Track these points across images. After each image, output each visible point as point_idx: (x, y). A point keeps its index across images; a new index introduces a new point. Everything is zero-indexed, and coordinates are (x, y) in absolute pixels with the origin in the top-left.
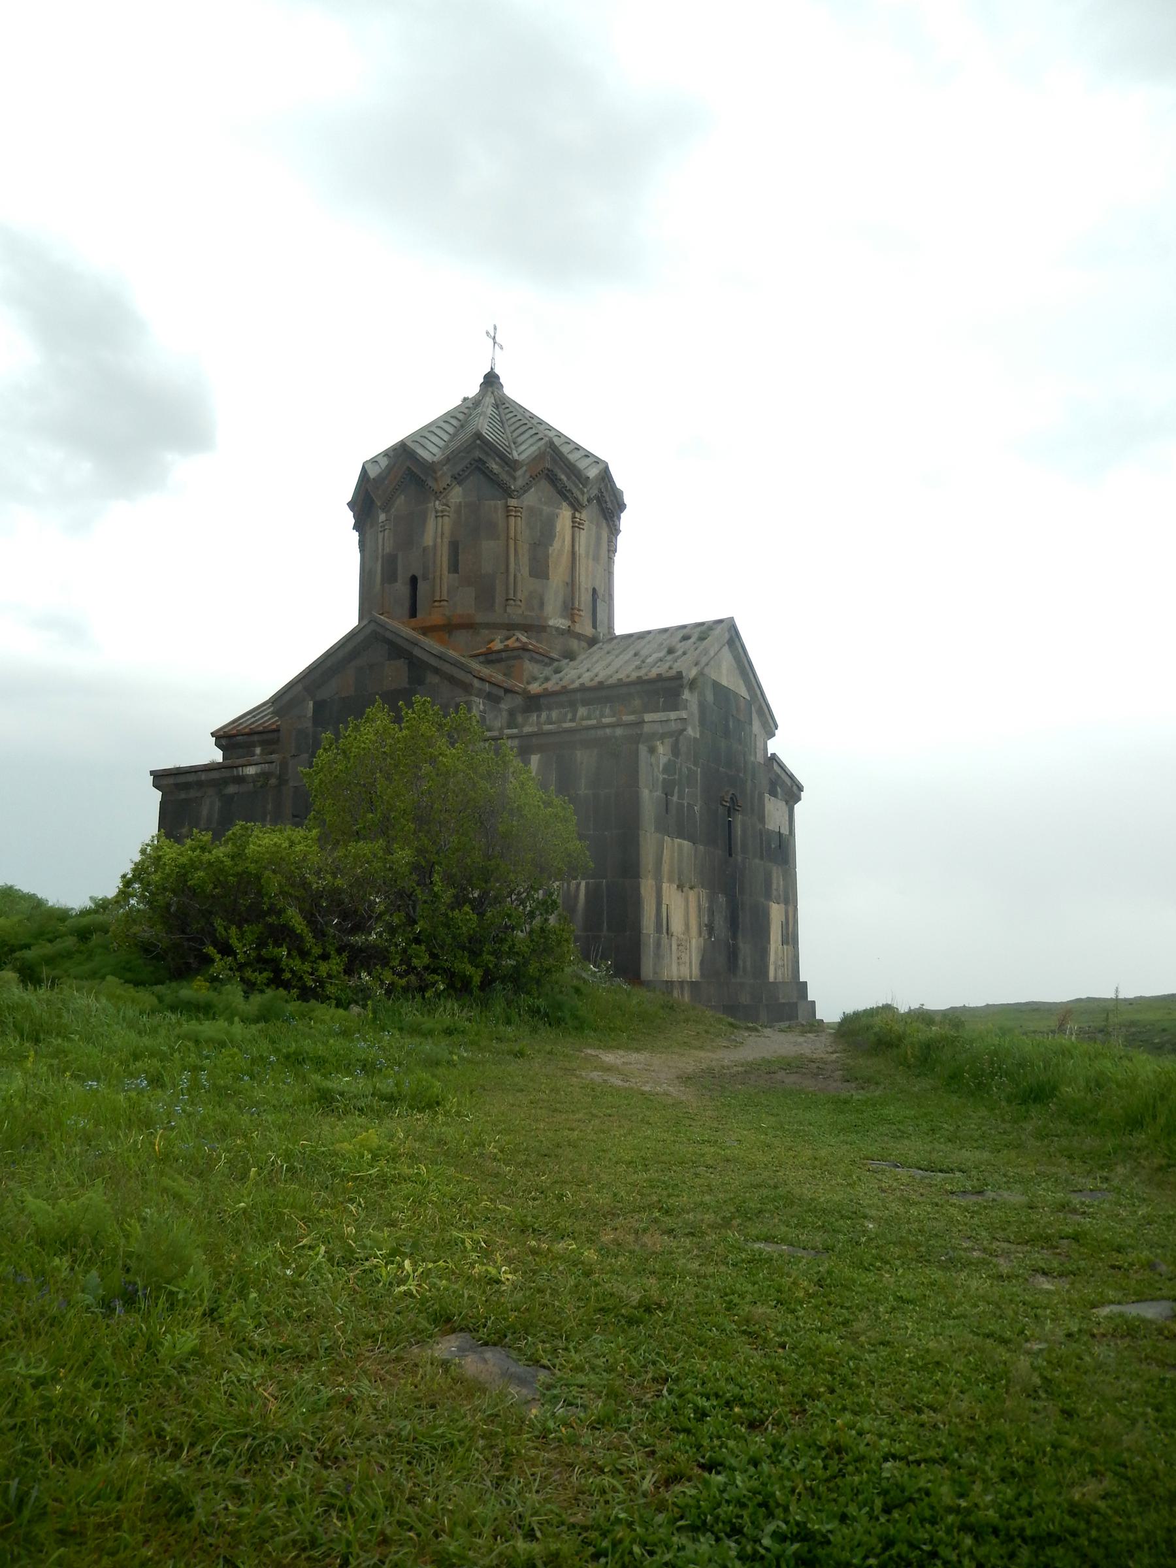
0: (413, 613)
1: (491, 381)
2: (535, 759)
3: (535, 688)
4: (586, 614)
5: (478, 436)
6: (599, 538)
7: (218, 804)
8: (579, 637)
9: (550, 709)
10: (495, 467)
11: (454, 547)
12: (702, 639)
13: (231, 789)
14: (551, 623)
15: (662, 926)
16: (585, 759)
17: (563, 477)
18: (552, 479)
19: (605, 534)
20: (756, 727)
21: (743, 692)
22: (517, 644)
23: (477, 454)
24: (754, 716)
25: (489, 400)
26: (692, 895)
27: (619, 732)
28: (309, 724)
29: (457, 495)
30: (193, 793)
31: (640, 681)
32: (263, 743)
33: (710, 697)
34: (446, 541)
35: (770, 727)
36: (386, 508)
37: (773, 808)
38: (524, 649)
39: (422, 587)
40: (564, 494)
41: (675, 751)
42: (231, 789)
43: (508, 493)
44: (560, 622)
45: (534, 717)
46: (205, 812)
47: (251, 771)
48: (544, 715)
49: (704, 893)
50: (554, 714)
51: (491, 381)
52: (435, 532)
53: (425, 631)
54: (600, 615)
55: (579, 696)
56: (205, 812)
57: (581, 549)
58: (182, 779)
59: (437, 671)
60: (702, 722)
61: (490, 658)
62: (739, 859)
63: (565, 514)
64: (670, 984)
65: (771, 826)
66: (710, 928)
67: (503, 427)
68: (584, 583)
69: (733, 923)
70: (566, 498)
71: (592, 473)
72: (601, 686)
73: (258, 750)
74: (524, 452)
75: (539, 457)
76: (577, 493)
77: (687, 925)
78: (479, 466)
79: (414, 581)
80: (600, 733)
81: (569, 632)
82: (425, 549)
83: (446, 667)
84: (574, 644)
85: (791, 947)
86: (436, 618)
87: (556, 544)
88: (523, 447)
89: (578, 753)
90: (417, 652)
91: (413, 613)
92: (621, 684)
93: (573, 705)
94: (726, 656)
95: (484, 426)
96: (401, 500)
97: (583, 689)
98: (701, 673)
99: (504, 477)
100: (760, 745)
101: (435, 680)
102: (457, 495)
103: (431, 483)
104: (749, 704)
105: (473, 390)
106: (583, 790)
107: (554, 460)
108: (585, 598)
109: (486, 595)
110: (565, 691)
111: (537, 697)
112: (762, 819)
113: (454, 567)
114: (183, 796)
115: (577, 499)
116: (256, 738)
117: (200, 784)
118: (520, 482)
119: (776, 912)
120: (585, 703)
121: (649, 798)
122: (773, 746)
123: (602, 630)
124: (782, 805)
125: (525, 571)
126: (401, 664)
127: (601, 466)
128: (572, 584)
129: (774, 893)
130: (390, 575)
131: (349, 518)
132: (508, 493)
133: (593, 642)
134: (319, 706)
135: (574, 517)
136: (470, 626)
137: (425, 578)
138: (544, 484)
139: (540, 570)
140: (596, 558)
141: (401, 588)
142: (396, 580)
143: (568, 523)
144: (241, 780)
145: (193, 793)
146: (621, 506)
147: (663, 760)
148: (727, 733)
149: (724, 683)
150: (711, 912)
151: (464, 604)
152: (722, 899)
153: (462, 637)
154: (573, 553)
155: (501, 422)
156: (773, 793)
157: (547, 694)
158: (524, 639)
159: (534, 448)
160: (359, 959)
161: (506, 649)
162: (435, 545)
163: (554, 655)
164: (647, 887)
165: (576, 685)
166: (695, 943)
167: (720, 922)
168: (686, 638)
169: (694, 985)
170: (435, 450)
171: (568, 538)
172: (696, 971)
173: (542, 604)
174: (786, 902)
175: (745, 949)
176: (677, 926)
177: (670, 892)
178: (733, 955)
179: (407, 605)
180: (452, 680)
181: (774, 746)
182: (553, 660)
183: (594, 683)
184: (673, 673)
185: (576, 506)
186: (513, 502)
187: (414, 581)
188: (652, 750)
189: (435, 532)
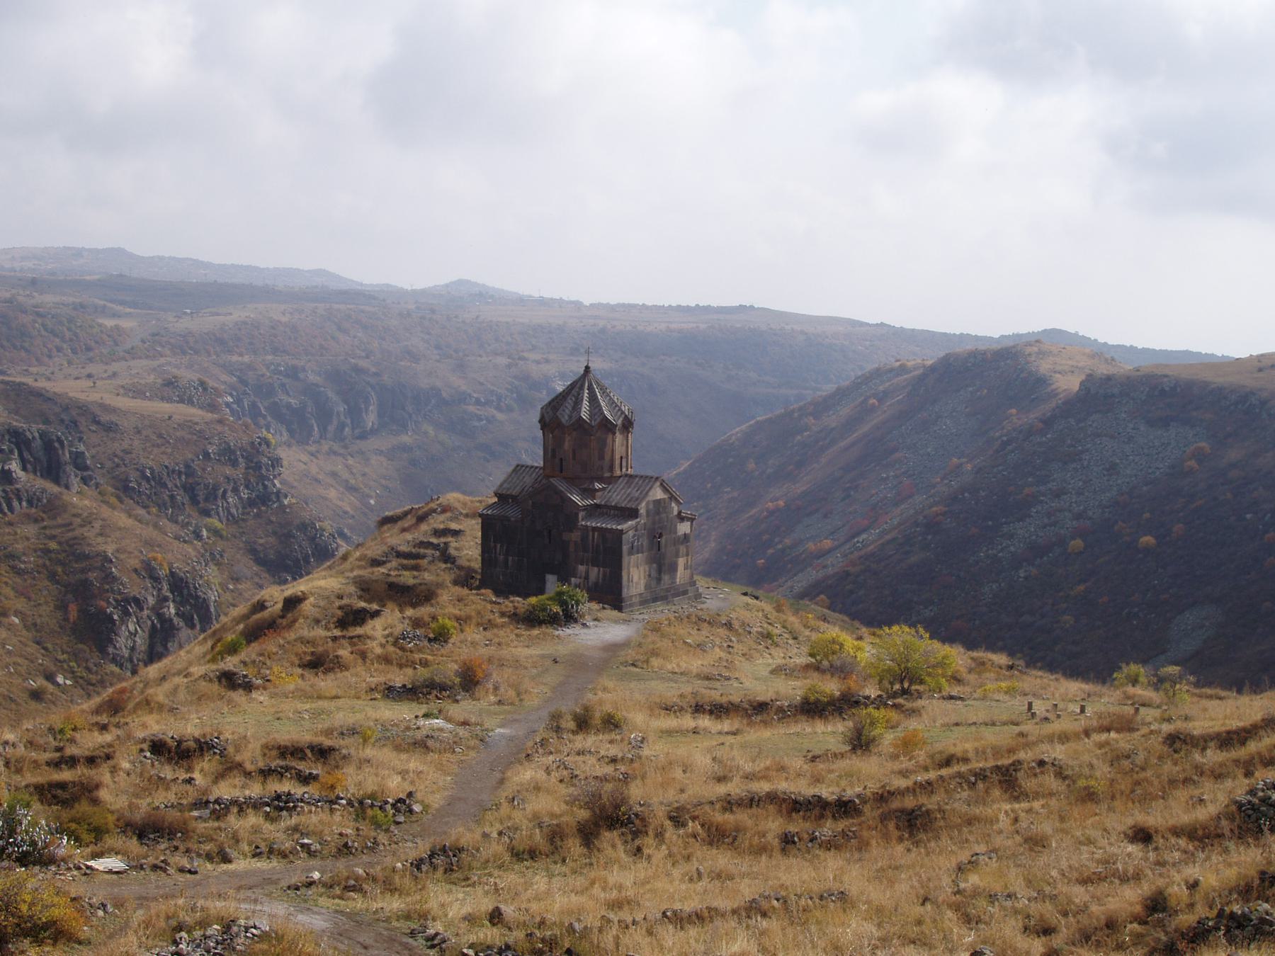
1: (587, 368)
11: (574, 451)
33: (651, 506)
51: (587, 368)
52: (567, 445)
54: (624, 464)
60: (648, 515)
62: (663, 550)
63: (610, 436)
69: (660, 571)
105: (582, 371)
108: (617, 462)
113: (574, 458)
119: (681, 562)
121: (625, 548)
128: (612, 460)
130: (554, 456)
131: (539, 426)
139: (602, 458)
141: (557, 461)
148: (658, 513)
166: (643, 582)
167: (654, 574)
175: (666, 578)
176: (635, 579)
178: (659, 580)
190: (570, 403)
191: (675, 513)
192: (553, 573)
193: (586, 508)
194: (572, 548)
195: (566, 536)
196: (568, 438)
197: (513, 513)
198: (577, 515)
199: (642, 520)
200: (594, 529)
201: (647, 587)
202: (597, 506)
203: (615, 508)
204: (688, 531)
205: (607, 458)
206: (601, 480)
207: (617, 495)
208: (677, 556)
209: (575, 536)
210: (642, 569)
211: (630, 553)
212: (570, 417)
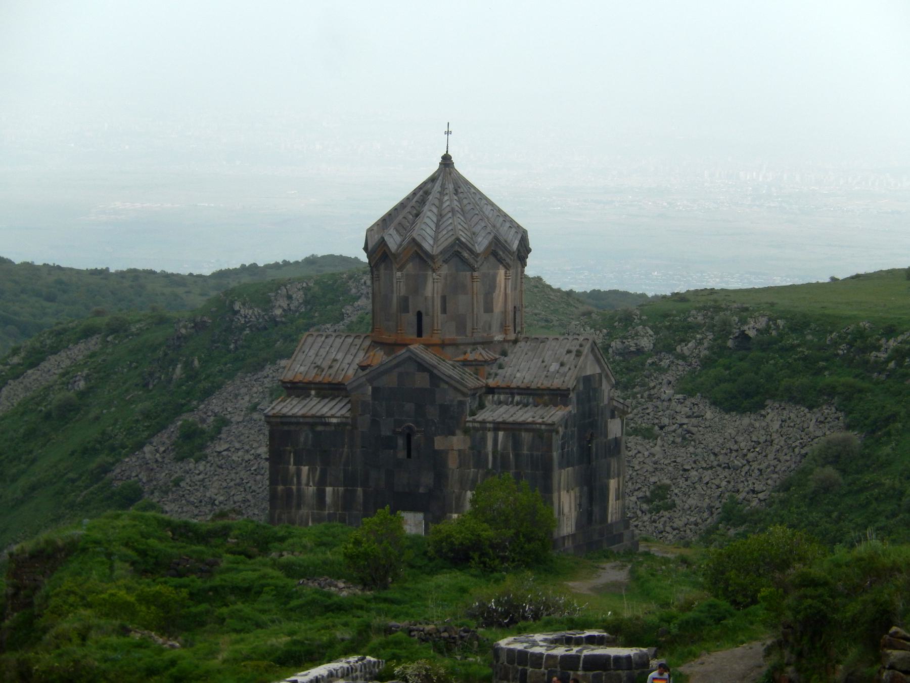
0: (420, 334)
1: (447, 161)
2: (501, 434)
3: (491, 382)
4: (511, 328)
5: (458, 239)
6: (517, 274)
7: (311, 436)
8: (508, 341)
9: (499, 393)
10: (466, 254)
11: (444, 299)
12: (579, 354)
13: (319, 428)
14: (496, 339)
15: (561, 512)
16: (526, 437)
17: (501, 253)
18: (495, 254)
19: (519, 269)
21: (598, 371)
22: (480, 358)
23: (456, 248)
24: (604, 381)
25: (450, 187)
26: (572, 493)
27: (543, 427)
28: (369, 399)
29: (445, 270)
30: (292, 428)
31: (548, 389)
32: (315, 389)
33: (581, 387)
34: (439, 296)
38: (486, 361)
39: (425, 320)
40: (501, 261)
41: (566, 428)
42: (319, 428)
43: (473, 269)
44: (499, 337)
45: (490, 397)
46: (302, 439)
48: (496, 397)
49: (577, 489)
50: (502, 397)
51: (447, 161)
52: (433, 287)
53: (428, 346)
55: (516, 391)
56: (302, 439)
57: (509, 291)
58: (284, 420)
59: (447, 383)
60: (578, 404)
61: (466, 363)
63: (502, 272)
64: (564, 538)
65: (611, 436)
66: (580, 505)
67: (465, 218)
69: (591, 499)
70: (502, 263)
71: (515, 246)
72: (528, 388)
73: (313, 392)
74: (482, 244)
75: (490, 244)
76: (508, 260)
77: (570, 508)
78: (458, 254)
79: (419, 315)
80: (534, 426)
81: (505, 341)
82: (426, 298)
83: (453, 382)
84: (506, 345)
85: (620, 501)
86: (436, 339)
87: (497, 292)
88: (480, 239)
89: (523, 434)
90: (435, 371)
91: (420, 334)
92: (538, 389)
93: (513, 395)
94: (591, 357)
95: (458, 227)
96: (410, 266)
97: (518, 388)
98: (578, 379)
99: (471, 261)
100: (606, 394)
101: (446, 386)
102: (445, 270)
103: (430, 263)
104: (600, 375)
106: (525, 451)
107: (496, 245)
109: (461, 327)
110: (508, 388)
111: (494, 388)
112: (606, 436)
113: (444, 311)
114: (286, 428)
115: (508, 264)
116: (313, 386)
117: (298, 424)
118: (479, 263)
119: (613, 484)
120: (519, 394)
121: (555, 455)
123: (518, 329)
124: (618, 421)
125: (482, 310)
126: (426, 375)
127: (519, 236)
129: (612, 474)
132: (473, 269)
133: (515, 342)
134: (375, 390)
135: (506, 273)
136: (455, 344)
137: (427, 314)
138: (492, 259)
139: (489, 309)
140: (515, 289)
141: (411, 317)
142: (408, 312)
143: (503, 277)
144: (329, 424)
145: (292, 428)
146: (529, 251)
147: (561, 433)
149: (588, 373)
150: (581, 497)
151: (450, 333)
152: (585, 488)
153: (449, 350)
154: (506, 294)
155: (462, 210)
156: (613, 417)
157: (498, 388)
158: (483, 352)
159: (486, 243)
160: (504, 559)
161: (476, 360)
162: (433, 297)
163: (497, 356)
164: (555, 495)
165: (513, 385)
166: (574, 514)
168: (569, 352)
169: (573, 536)
170: (431, 242)
171: (503, 285)
172: (574, 528)
173: (490, 328)
174: (619, 476)
175: (596, 509)
176: (566, 510)
177: (564, 494)
178: (590, 514)
179: (416, 328)
180: (456, 389)
182: (496, 360)
183: (522, 386)
184: (564, 387)
185: (507, 267)
186: (476, 274)
187: (419, 315)
188: (557, 432)
189: (433, 287)
190: (429, 215)
191: (606, 402)
192: (413, 509)
193: (474, 392)
194: (452, 463)
195: (439, 443)
197: (333, 410)
198: (462, 404)
199: (571, 409)
200: (498, 426)
201: (579, 525)
202: (491, 390)
203: (526, 391)
204: (619, 435)
205: (498, 307)
206: (487, 343)
207: (522, 369)
208: (609, 477)
209: (458, 442)
210: (572, 493)
211: (561, 467)
212: (436, 239)
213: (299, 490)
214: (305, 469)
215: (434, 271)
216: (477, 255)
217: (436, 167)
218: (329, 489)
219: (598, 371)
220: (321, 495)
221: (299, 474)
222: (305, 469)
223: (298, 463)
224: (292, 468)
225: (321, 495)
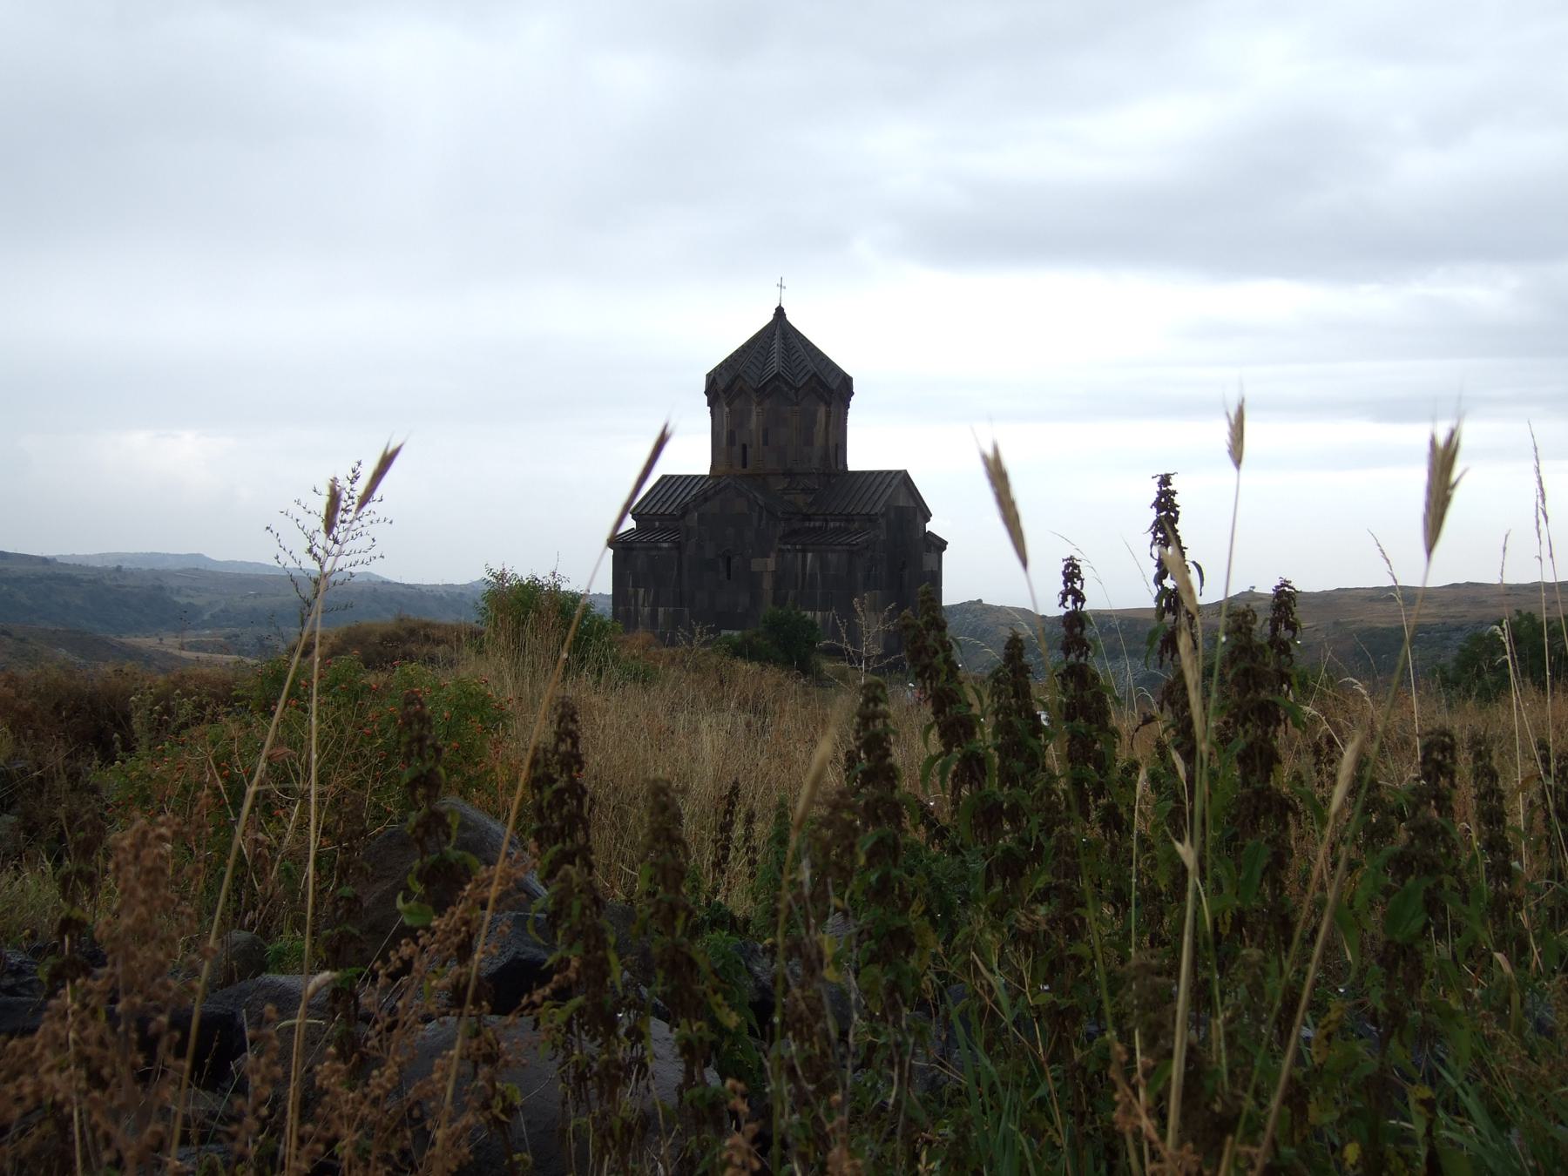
1: (780, 312)
2: (810, 555)
20: (919, 518)
21: (912, 504)
35: (927, 516)
36: (728, 405)
37: (928, 559)
42: (654, 553)
47: (665, 545)
51: (780, 312)
65: (927, 569)
68: (831, 443)
79: (744, 447)
91: (744, 466)
105: (770, 318)
113: (766, 443)
122: (929, 527)
141: (737, 449)
181: (929, 527)
185: (828, 404)
187: (744, 447)
195: (756, 565)
196: (755, 410)
213: (636, 610)
214: (641, 591)
215: (759, 404)
216: (797, 390)
217: (767, 317)
218: (661, 610)
219: (912, 504)
220: (654, 615)
221: (636, 594)
222: (641, 591)
223: (636, 586)
224: (631, 590)
225: (654, 615)
